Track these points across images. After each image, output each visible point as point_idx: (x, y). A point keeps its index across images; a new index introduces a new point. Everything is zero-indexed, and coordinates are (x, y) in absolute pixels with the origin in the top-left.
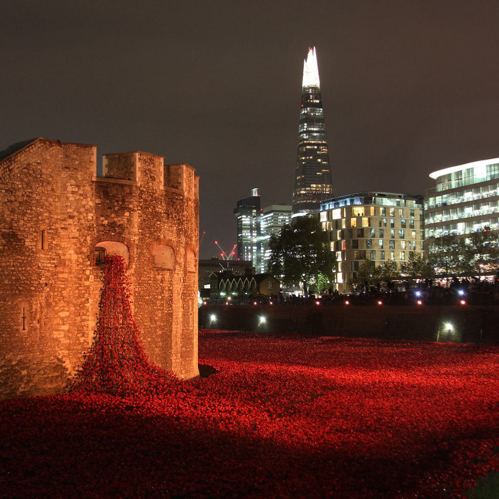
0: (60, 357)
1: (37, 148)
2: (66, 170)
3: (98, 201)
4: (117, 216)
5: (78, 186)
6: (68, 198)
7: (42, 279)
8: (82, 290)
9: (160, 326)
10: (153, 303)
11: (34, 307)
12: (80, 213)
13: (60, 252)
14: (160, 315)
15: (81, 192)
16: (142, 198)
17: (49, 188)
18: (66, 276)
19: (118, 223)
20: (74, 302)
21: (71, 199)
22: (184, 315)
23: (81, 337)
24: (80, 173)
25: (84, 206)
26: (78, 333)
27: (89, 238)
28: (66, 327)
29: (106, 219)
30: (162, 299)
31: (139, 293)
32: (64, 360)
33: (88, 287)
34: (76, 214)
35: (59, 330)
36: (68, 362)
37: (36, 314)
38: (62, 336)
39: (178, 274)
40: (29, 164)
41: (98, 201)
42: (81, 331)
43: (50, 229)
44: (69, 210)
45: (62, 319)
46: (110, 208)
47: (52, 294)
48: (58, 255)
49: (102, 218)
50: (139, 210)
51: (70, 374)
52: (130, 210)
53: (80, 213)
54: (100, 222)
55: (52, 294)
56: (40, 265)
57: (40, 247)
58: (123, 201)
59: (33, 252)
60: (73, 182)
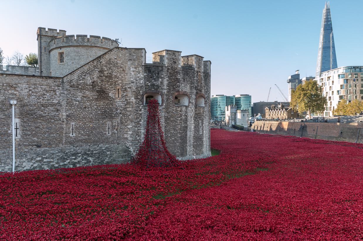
0: (128, 146)
1: (114, 51)
2: (130, 61)
3: (145, 74)
4: (155, 81)
5: (136, 68)
6: (131, 74)
7: (118, 111)
8: (138, 116)
9: (180, 133)
10: (175, 122)
11: (114, 123)
12: (137, 80)
13: (128, 98)
14: (179, 127)
16: (168, 72)
17: (122, 69)
18: (130, 109)
19: (156, 84)
20: (134, 121)
21: (133, 74)
22: (195, 127)
23: (138, 137)
24: (136, 62)
25: (139, 77)
26: (136, 135)
28: (131, 133)
29: (149, 83)
30: (180, 119)
31: (167, 117)
32: (130, 147)
33: (141, 114)
34: (135, 81)
35: (127, 134)
36: (131, 148)
37: (115, 127)
38: (129, 136)
39: (191, 108)
40: (110, 59)
41: (145, 74)
42: (138, 134)
43: (122, 88)
44: (132, 79)
45: (129, 128)
46: (152, 78)
47: (123, 117)
48: (126, 100)
49: (147, 82)
50: (167, 78)
51: (132, 154)
52: (162, 78)
54: (146, 84)
55: (123, 117)
56: (117, 104)
57: (117, 96)
58: (158, 74)
59: (113, 99)
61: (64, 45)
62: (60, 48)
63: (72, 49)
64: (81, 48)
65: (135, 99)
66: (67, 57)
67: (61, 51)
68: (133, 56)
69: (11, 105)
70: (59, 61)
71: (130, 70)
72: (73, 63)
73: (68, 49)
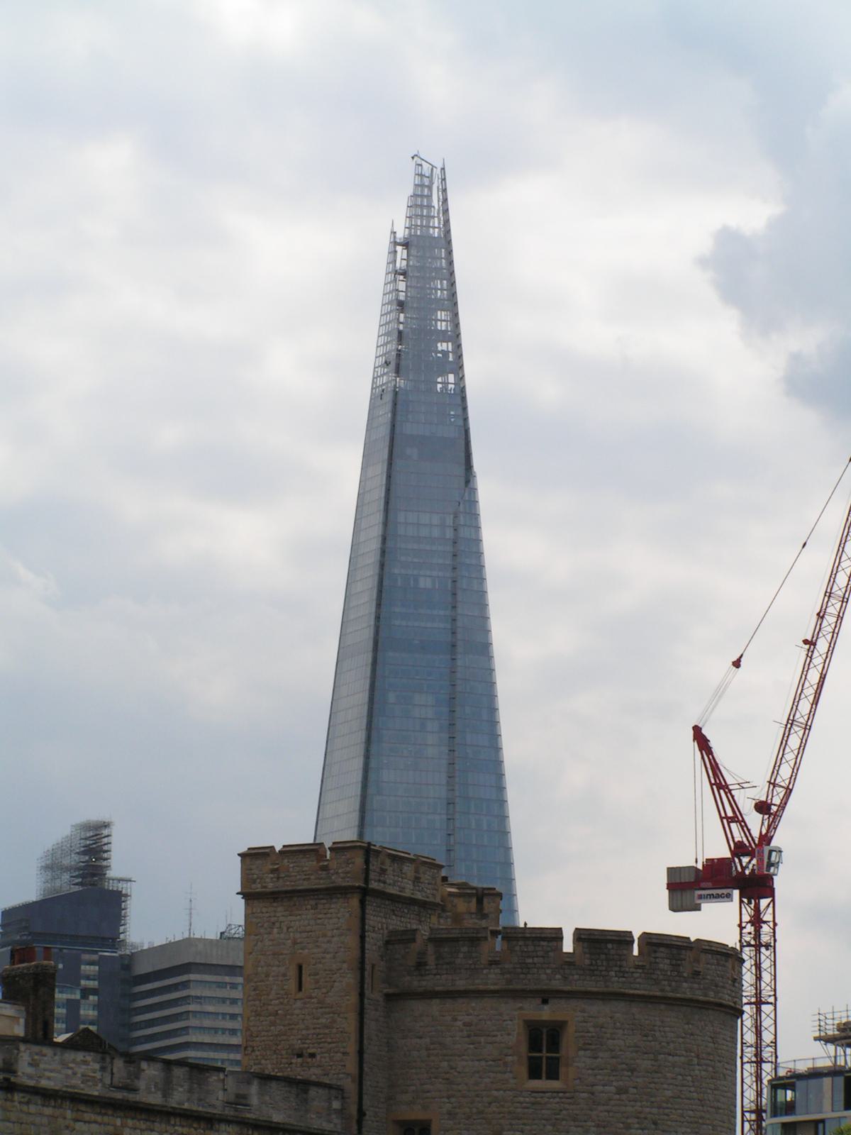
61: (578, 984)
62: (546, 997)
63: (619, 1009)
64: (663, 1007)
66: (588, 1053)
67: (546, 1013)
70: (524, 1071)
72: (621, 1091)
73: (595, 1008)
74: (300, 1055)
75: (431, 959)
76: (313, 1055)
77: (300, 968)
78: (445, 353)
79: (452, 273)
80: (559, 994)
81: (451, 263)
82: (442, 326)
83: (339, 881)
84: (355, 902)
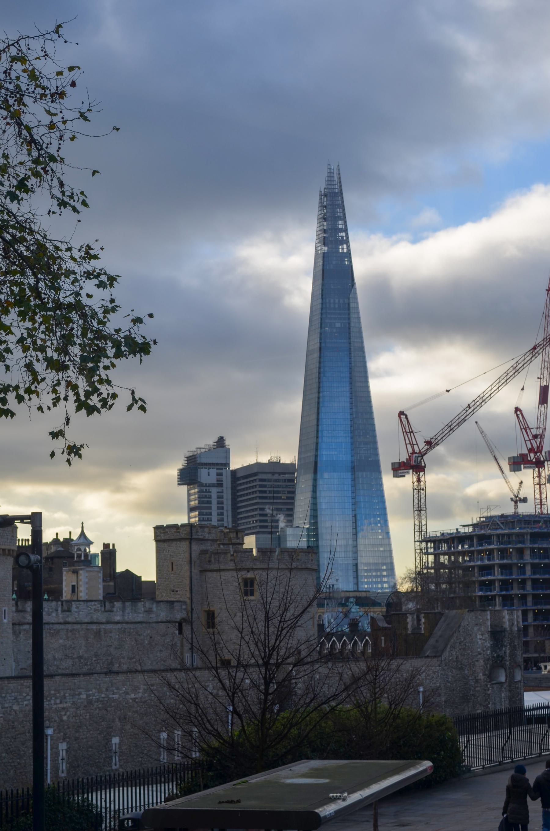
4: (500, 651)
5: (482, 635)
6: (478, 643)
15: (484, 638)
21: (480, 643)
27: (488, 666)
33: (489, 695)
34: (482, 652)
44: (479, 650)
53: (484, 651)
58: (502, 641)
60: (480, 633)
61: (259, 565)
65: (483, 675)
67: (250, 575)
68: (479, 619)
69: (419, 692)
71: (476, 638)
74: (173, 591)
75: (213, 559)
76: (177, 591)
77: (172, 563)
78: (342, 237)
79: (344, 206)
80: (253, 569)
81: (343, 202)
82: (340, 227)
83: (183, 536)
84: (188, 543)
